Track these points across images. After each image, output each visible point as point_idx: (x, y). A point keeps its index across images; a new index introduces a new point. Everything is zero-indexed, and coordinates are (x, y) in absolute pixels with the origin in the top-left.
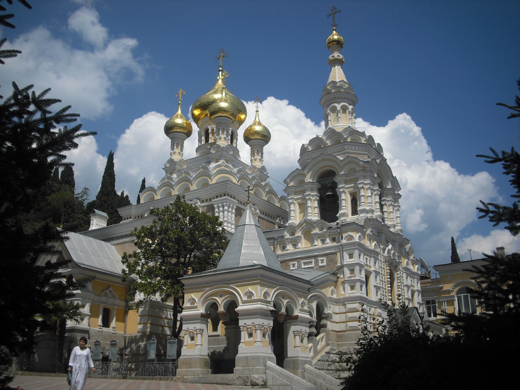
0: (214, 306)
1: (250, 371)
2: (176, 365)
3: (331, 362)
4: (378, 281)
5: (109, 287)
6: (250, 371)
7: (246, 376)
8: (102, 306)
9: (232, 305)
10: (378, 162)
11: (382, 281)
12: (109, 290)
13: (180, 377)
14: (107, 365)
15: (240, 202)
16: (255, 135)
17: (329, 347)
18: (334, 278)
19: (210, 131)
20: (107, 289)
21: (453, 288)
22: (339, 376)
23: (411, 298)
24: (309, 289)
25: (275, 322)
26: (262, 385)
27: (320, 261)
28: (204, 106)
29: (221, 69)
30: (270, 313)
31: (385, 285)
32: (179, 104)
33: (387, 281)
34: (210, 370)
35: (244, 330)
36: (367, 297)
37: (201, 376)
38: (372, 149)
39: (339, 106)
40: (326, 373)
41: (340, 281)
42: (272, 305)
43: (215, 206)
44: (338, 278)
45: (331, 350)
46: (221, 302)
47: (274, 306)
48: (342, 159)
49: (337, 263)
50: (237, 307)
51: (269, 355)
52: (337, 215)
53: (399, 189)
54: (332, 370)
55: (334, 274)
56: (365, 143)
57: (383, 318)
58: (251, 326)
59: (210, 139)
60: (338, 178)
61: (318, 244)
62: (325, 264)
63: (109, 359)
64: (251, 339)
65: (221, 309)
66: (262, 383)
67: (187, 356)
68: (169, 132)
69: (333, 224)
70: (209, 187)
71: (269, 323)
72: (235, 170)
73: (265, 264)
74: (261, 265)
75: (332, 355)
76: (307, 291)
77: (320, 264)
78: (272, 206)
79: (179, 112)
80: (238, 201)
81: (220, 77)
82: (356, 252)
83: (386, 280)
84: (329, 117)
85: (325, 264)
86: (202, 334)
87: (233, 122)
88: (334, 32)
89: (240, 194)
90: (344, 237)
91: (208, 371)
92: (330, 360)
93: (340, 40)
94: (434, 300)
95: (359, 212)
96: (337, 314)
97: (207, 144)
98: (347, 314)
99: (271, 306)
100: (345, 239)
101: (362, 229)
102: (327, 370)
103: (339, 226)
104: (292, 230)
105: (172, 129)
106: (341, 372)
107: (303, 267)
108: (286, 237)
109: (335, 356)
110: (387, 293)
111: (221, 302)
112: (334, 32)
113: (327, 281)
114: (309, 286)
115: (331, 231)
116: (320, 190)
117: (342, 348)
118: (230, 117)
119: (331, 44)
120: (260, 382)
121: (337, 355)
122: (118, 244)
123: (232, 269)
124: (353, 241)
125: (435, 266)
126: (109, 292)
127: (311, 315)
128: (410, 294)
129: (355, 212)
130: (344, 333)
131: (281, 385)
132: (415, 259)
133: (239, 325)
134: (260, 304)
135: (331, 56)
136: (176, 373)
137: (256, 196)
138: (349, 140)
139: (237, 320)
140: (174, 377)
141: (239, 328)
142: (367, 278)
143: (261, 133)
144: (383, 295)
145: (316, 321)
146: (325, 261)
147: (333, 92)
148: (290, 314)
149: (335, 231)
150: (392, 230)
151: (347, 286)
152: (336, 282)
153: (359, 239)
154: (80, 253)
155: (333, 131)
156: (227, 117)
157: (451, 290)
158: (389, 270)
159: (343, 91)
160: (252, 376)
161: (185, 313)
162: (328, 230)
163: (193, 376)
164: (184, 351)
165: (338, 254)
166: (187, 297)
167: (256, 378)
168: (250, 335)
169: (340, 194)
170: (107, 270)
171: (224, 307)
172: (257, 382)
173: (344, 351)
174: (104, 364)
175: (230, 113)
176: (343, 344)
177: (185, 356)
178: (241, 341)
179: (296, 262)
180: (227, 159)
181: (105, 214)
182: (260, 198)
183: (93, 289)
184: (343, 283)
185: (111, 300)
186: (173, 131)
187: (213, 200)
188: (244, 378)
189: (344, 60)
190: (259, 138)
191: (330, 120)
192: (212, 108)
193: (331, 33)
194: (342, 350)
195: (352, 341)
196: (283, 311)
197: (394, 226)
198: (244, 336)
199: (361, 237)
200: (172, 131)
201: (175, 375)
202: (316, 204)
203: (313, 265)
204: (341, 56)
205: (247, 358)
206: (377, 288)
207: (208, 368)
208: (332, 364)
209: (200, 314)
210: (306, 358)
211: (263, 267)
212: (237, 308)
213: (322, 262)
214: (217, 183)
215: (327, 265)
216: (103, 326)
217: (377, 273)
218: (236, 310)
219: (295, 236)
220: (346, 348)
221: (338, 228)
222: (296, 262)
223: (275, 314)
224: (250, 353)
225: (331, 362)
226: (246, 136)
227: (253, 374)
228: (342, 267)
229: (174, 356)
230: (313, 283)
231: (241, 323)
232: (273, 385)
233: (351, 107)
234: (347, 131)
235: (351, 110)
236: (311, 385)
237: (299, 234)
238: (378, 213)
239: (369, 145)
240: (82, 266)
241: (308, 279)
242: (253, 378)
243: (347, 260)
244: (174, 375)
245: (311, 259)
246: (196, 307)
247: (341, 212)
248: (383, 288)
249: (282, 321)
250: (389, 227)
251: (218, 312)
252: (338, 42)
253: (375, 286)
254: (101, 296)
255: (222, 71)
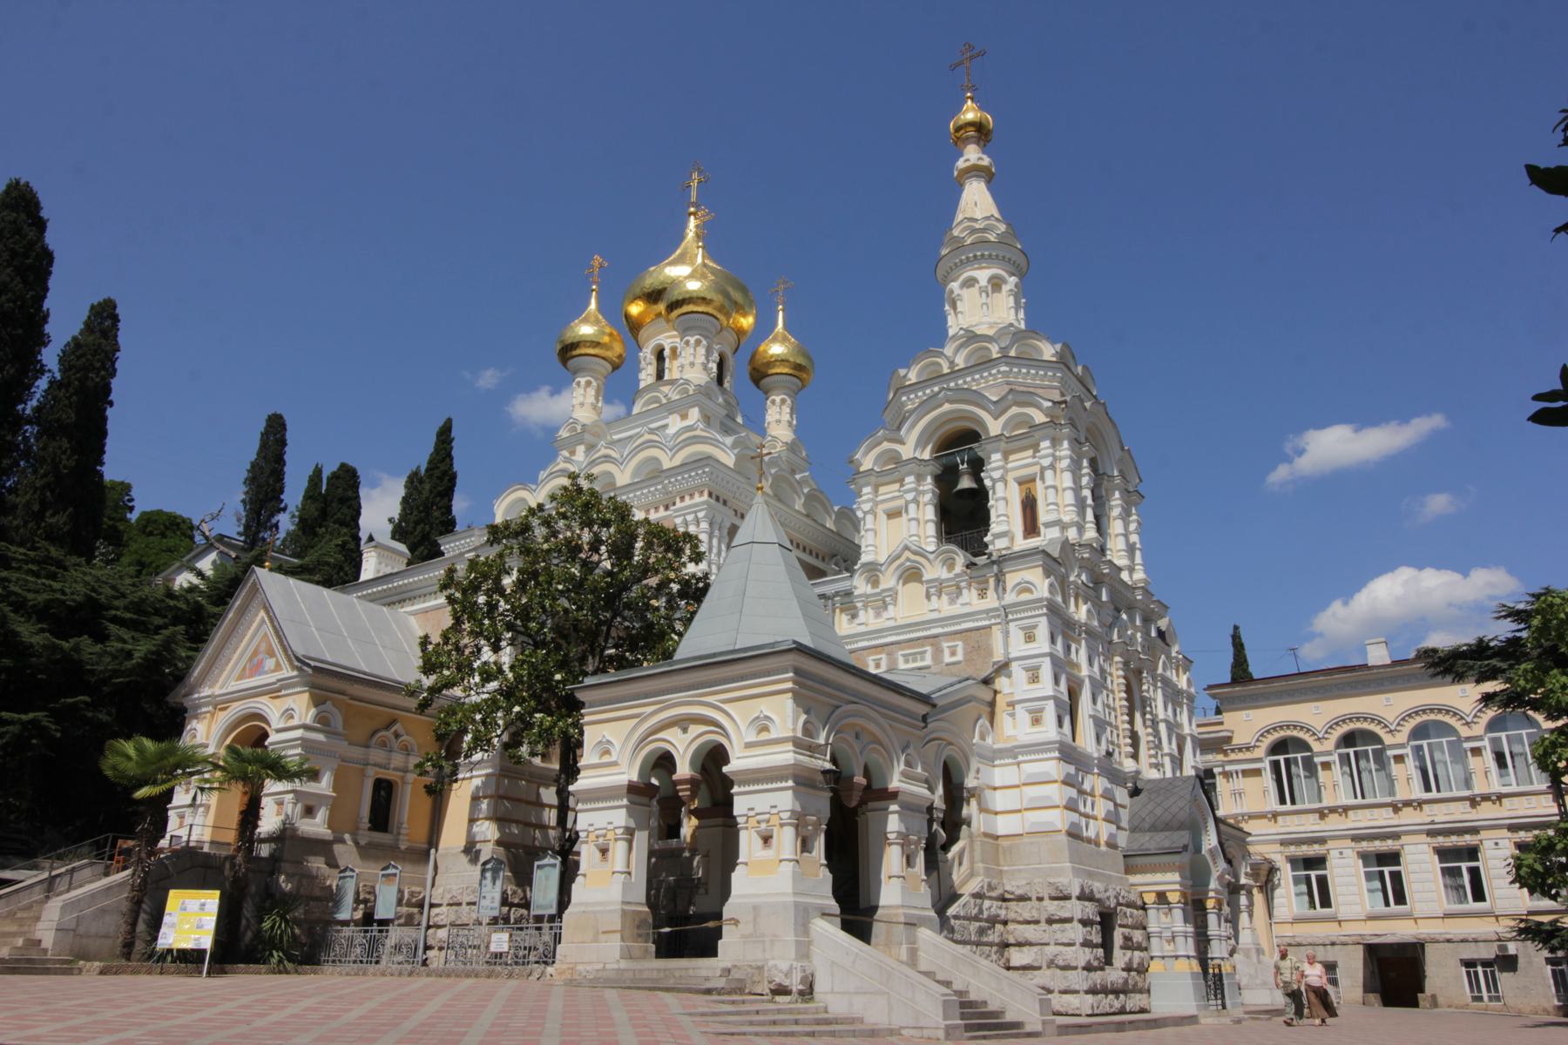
0: (665, 761)
1: (764, 950)
2: (556, 934)
3: (987, 921)
4: (1099, 706)
5: (393, 722)
6: (764, 950)
7: (753, 964)
8: (372, 774)
9: (714, 757)
10: (1088, 408)
11: (1108, 706)
12: (393, 729)
13: (565, 966)
14: (368, 935)
15: (739, 515)
16: (778, 363)
17: (980, 879)
18: (986, 694)
19: (667, 353)
20: (388, 727)
21: (1258, 740)
22: (1008, 960)
23: (1176, 753)
24: (924, 718)
25: (837, 804)
26: (801, 993)
27: (947, 652)
28: (653, 292)
29: (692, 209)
30: (820, 778)
31: (1116, 717)
32: (593, 290)
33: (1121, 707)
34: (653, 947)
35: (747, 828)
36: (1073, 744)
37: (623, 964)
38: (1070, 375)
39: (983, 275)
40: (975, 953)
41: (1001, 701)
42: (828, 757)
43: (678, 521)
44: (996, 692)
45: (985, 887)
46: (684, 747)
47: (834, 760)
48: (994, 399)
49: (991, 654)
50: (726, 761)
51: (819, 901)
52: (986, 539)
53: (1138, 481)
54: (991, 944)
55: (987, 682)
56: (1054, 359)
57: (1116, 805)
58: (767, 816)
59: (667, 371)
60: (987, 446)
61: (944, 606)
62: (959, 657)
63: (376, 917)
64: (769, 854)
65: (684, 770)
66: (801, 987)
67: (587, 904)
68: (568, 355)
69: (982, 560)
70: (664, 475)
71: (822, 804)
72: (729, 440)
73: (807, 641)
74: (795, 642)
75: (987, 903)
76: (918, 720)
77: (948, 659)
78: (819, 528)
79: (593, 305)
80: (736, 511)
81: (692, 222)
82: (1043, 629)
83: (1118, 704)
84: (959, 303)
85: (959, 657)
86: (630, 842)
87: (721, 330)
88: (969, 102)
89: (741, 494)
90: (1009, 585)
91: (646, 950)
92: (986, 914)
93: (984, 122)
94: (1212, 770)
95: (1042, 529)
96: (995, 789)
97: (660, 383)
98: (1025, 789)
99: (824, 760)
100: (1012, 590)
101: (1056, 566)
102: (978, 944)
103: (994, 558)
104: (873, 571)
105: (575, 349)
106: (1012, 949)
107: (902, 665)
108: (856, 593)
109: (996, 903)
110: (1121, 737)
111: (684, 747)
112: (969, 102)
113: (970, 701)
114: (922, 709)
115: (975, 574)
116: (938, 480)
117: (1013, 883)
118: (715, 313)
119: (962, 131)
120: (795, 984)
121: (1000, 903)
122: (426, 611)
123: (714, 655)
124: (1036, 595)
125: (1210, 687)
126: (393, 737)
127: (931, 789)
128: (1174, 746)
129: (1031, 528)
130: (1017, 841)
131: (857, 993)
132: (1180, 656)
133: (735, 813)
134: (795, 752)
135: (962, 160)
136: (554, 957)
137: (780, 500)
138: (1012, 353)
139: (728, 803)
140: (550, 970)
141: (735, 817)
142: (1073, 694)
143: (791, 359)
144: (1112, 743)
145: (944, 807)
146: (960, 651)
147: (969, 242)
148: (876, 786)
149: (985, 571)
150: (1125, 576)
151: (1022, 713)
152: (992, 704)
153: (1050, 592)
154: (316, 632)
155: (972, 335)
156: (707, 314)
157: (1252, 744)
158: (1125, 678)
159: (993, 239)
160: (771, 963)
161: (582, 783)
162: (969, 571)
163: (602, 966)
164: (578, 889)
165: (997, 635)
166: (591, 736)
167: (781, 971)
168: (767, 839)
169: (993, 487)
170: (392, 677)
171: (692, 763)
172: (786, 983)
173: (1019, 892)
174: (362, 934)
175: (717, 304)
176: (1014, 870)
177: (581, 904)
178: (739, 861)
179: (883, 656)
180: (710, 414)
181: (402, 548)
182: (788, 506)
183: (344, 729)
184: (1012, 704)
185: (397, 759)
186: (578, 352)
187: (672, 508)
188: (749, 970)
189: (993, 170)
190: (786, 370)
191: (962, 313)
192: (676, 295)
193: (958, 108)
194: (1013, 889)
195: (1040, 864)
196: (860, 779)
197: (1131, 570)
198: (748, 842)
199: (1055, 588)
200: (575, 353)
201: (554, 962)
202: (930, 513)
203: (928, 661)
204: (986, 161)
205: (756, 908)
206: (1100, 725)
207: (646, 942)
208: (989, 928)
209: (626, 783)
210: (923, 908)
211: (800, 649)
212: (729, 765)
213: (953, 654)
214: (681, 465)
215: (965, 658)
216: (370, 829)
217: (1099, 686)
218: (725, 769)
219: (882, 586)
220: (1024, 882)
221: (993, 562)
222: (883, 656)
223: (836, 780)
224: (765, 895)
225: (987, 921)
226: (754, 369)
227: (773, 959)
228: (1003, 668)
229: (551, 907)
230: (936, 702)
231: (740, 806)
232: (832, 992)
233: (1013, 280)
234: (1005, 334)
235: (1013, 288)
236: (946, 995)
237: (888, 580)
238: (1091, 533)
239: (1062, 366)
240: (313, 663)
241: (924, 690)
242: (774, 972)
243: (1018, 647)
244: (550, 961)
245: (923, 646)
246: (615, 764)
247: (995, 528)
248: (1110, 724)
249: (854, 804)
250: (1120, 569)
251: (675, 777)
252: (979, 126)
253: (1095, 718)
254: (367, 747)
255: (694, 214)
